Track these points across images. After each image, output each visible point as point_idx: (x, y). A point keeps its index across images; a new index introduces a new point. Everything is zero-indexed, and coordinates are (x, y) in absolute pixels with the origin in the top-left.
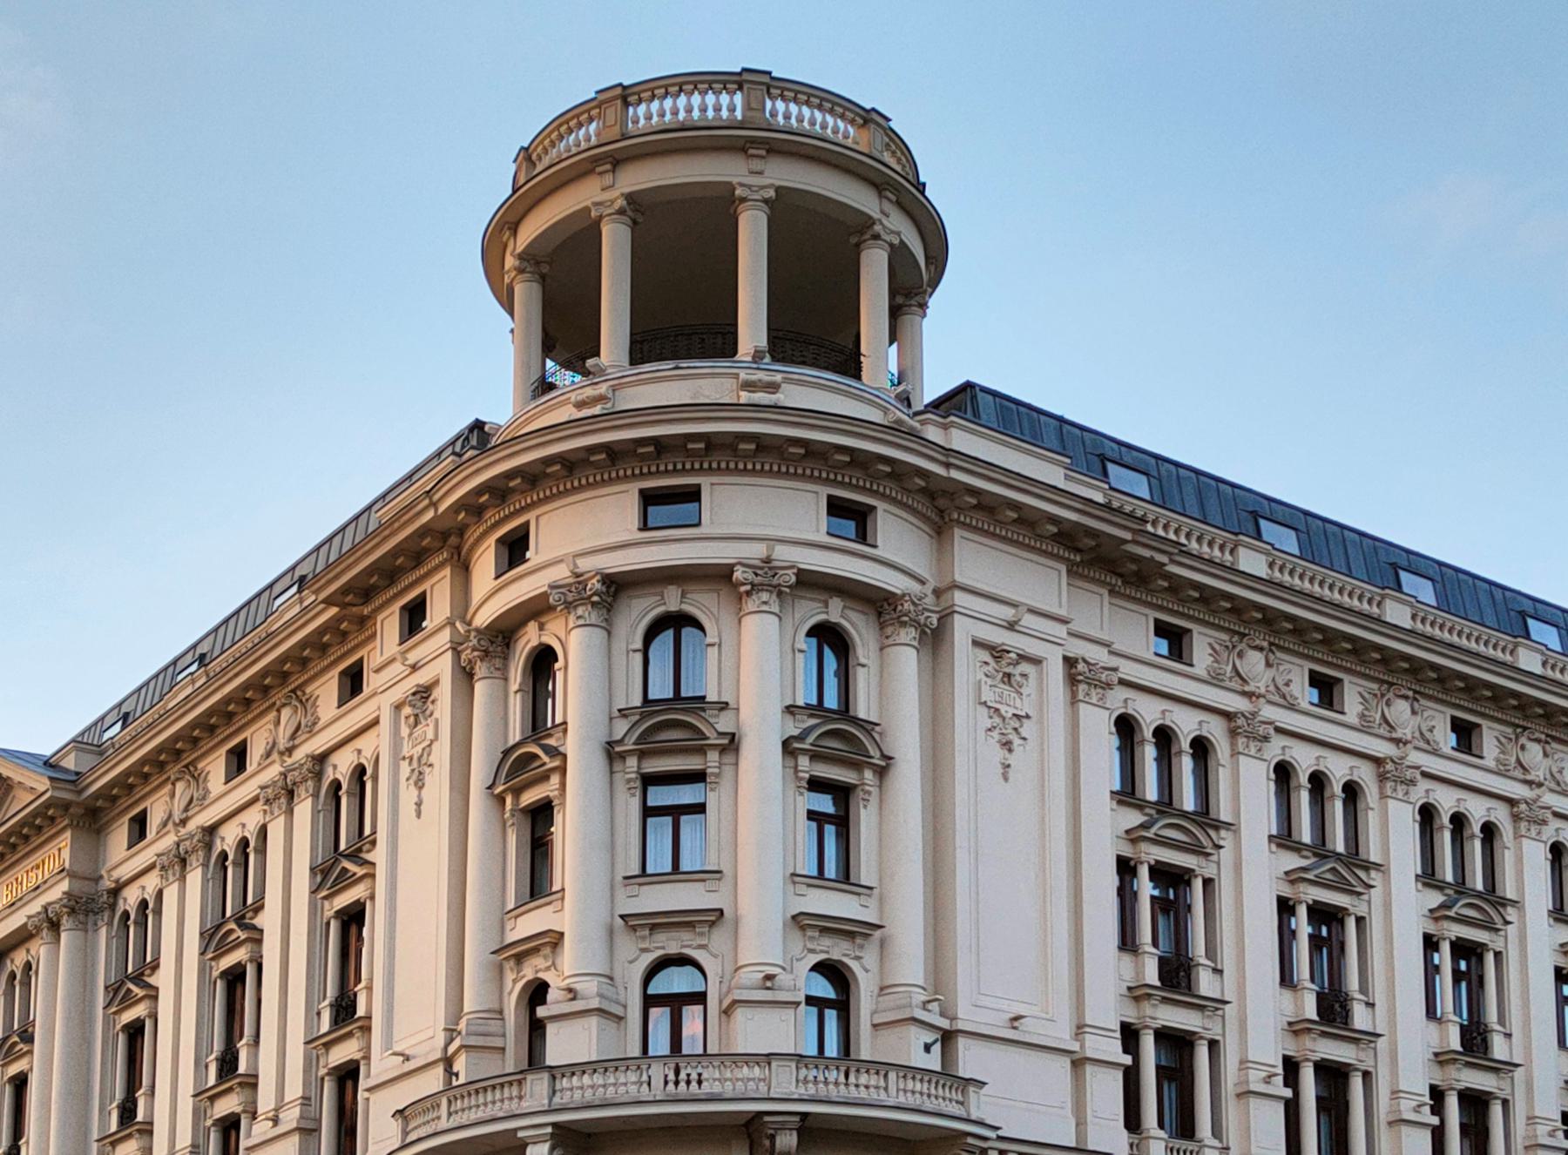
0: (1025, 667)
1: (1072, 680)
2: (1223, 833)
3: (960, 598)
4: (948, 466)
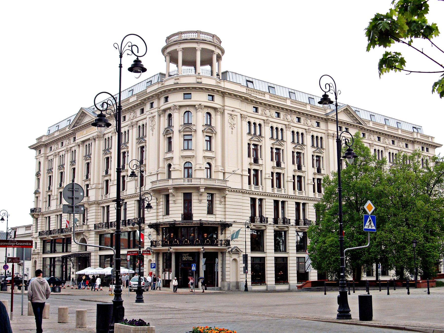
0: (235, 117)
1: (241, 117)
2: (263, 138)
3: (226, 108)
4: (224, 90)
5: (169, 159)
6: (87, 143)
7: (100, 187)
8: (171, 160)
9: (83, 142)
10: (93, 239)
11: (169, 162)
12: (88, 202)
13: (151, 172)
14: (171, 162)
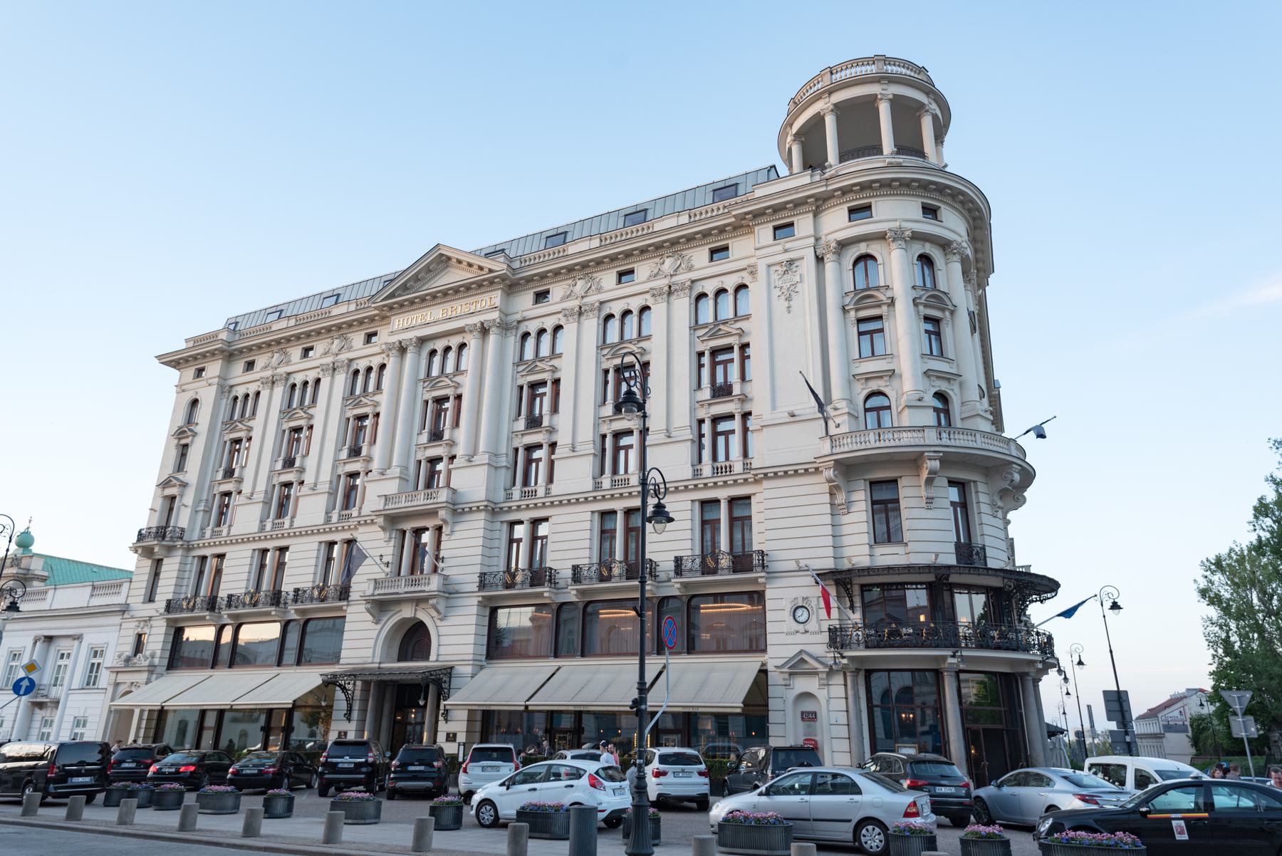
5: (881, 377)
6: (439, 345)
7: (505, 464)
8: (885, 378)
9: (422, 341)
10: (473, 619)
11: (874, 385)
12: (454, 504)
13: (796, 413)
14: (887, 386)
